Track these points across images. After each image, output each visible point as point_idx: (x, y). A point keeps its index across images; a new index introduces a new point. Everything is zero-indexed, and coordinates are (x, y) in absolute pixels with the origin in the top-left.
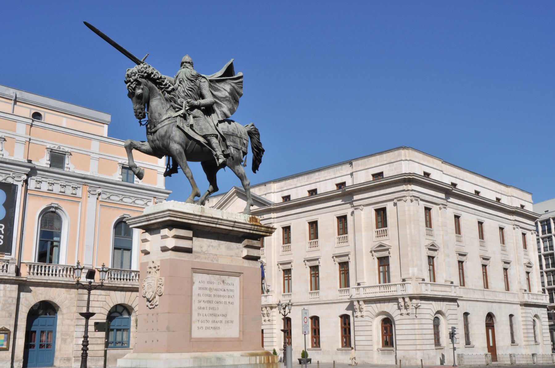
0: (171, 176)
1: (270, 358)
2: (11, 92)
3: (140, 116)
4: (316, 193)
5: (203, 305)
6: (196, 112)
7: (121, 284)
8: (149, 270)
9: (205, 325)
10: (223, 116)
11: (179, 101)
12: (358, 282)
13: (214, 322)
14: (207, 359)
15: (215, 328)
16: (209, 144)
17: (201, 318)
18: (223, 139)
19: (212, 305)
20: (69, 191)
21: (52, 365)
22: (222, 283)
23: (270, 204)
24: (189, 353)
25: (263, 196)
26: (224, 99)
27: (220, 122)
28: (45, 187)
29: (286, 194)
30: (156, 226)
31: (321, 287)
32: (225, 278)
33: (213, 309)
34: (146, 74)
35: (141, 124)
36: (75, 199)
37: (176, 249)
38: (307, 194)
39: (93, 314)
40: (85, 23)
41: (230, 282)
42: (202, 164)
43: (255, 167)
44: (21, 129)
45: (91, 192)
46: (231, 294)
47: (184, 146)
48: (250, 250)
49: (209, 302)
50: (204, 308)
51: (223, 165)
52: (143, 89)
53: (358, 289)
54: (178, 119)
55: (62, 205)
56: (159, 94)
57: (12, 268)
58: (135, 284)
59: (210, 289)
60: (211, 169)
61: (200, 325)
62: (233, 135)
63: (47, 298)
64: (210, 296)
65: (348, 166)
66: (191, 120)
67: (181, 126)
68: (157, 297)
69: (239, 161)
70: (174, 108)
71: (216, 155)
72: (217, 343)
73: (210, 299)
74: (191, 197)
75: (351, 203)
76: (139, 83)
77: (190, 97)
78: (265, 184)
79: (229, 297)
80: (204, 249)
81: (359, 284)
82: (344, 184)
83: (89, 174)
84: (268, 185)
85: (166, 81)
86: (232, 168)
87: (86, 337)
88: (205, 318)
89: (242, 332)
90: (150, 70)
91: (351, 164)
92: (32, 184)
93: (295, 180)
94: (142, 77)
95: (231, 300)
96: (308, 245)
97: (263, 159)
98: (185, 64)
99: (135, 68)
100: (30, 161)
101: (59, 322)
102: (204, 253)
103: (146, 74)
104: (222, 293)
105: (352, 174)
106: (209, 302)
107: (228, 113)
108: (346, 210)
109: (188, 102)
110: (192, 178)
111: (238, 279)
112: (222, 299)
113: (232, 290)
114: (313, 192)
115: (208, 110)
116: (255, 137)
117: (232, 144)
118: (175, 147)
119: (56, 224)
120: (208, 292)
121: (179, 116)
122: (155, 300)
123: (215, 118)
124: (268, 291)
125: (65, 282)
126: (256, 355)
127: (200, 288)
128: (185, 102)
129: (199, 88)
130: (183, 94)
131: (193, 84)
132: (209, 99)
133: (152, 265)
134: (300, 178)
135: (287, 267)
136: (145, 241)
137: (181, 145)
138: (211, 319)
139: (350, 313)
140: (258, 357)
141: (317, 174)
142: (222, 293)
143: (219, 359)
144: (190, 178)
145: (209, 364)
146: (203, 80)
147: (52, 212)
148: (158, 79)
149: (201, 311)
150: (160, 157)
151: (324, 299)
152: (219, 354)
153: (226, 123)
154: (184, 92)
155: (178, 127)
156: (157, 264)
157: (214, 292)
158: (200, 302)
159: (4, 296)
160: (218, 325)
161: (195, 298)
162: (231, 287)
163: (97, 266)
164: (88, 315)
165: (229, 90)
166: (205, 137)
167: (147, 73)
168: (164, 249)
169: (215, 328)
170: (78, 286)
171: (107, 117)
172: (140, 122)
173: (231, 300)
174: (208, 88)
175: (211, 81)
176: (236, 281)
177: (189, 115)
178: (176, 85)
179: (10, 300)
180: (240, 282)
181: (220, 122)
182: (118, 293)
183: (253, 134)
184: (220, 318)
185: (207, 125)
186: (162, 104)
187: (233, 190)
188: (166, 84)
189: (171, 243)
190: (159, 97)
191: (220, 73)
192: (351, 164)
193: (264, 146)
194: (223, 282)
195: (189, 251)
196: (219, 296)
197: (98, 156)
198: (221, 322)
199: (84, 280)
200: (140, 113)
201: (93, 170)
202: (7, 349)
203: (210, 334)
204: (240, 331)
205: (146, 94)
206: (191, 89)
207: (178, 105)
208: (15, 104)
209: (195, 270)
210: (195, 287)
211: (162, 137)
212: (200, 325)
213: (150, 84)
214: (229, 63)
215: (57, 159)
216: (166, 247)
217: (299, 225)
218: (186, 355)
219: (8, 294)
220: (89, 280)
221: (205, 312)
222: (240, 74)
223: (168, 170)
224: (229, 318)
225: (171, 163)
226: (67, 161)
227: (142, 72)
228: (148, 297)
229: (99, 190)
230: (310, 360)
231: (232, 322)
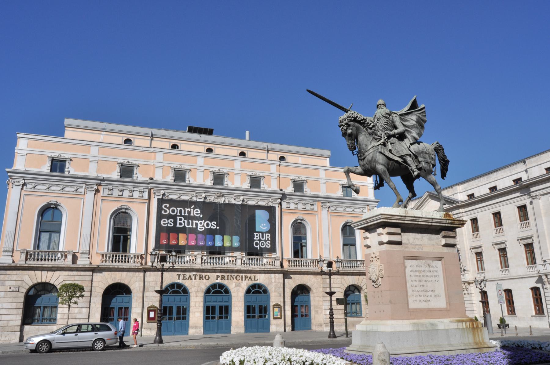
1: (475, 324)
2: (265, 145)
3: (352, 148)
4: (496, 189)
5: (415, 283)
6: (392, 139)
7: (351, 270)
8: (371, 259)
9: (418, 298)
11: (379, 134)
12: (544, 259)
13: (425, 296)
14: (423, 325)
15: (426, 301)
16: (405, 162)
17: (415, 293)
18: (415, 157)
19: (422, 284)
20: (308, 207)
21: (310, 329)
23: (458, 202)
24: (409, 321)
25: (452, 197)
26: (413, 127)
27: (412, 144)
28: (292, 206)
29: (470, 192)
30: (373, 227)
31: (510, 265)
32: (430, 262)
33: (423, 286)
36: (313, 212)
37: (390, 243)
38: (488, 191)
39: (334, 293)
40: (308, 91)
41: (434, 265)
42: (401, 177)
43: (443, 175)
44: (274, 169)
46: (436, 274)
48: (448, 239)
50: (416, 286)
51: (418, 176)
52: (352, 129)
53: (544, 265)
54: (380, 146)
55: (305, 217)
56: (364, 131)
57: (278, 263)
59: (419, 271)
60: (409, 180)
61: (414, 298)
62: (423, 152)
63: (302, 283)
64: (419, 276)
65: (522, 164)
66: (389, 146)
67: (382, 151)
68: (380, 279)
69: (430, 172)
70: (376, 139)
71: (412, 169)
72: (430, 313)
73: (420, 279)
74: (396, 203)
75: (529, 194)
76: (349, 126)
77: (387, 129)
78: (451, 187)
79: (435, 276)
80: (411, 241)
81: (545, 261)
82: (520, 179)
83: (320, 194)
84: (454, 188)
85: (367, 121)
86: (425, 177)
87: (331, 309)
88: (417, 294)
89: (449, 303)
90: (355, 115)
91: (524, 162)
92: (284, 205)
93: (477, 181)
94: (351, 121)
95: (436, 279)
96: (494, 232)
97: (449, 167)
99: (345, 115)
100: (281, 190)
101: (312, 299)
102: (411, 244)
104: (429, 274)
105: (526, 171)
106: (419, 281)
107: (417, 137)
108: (525, 200)
109: (385, 134)
110: (395, 189)
111: (440, 262)
112: (429, 279)
113: (436, 271)
114: (493, 189)
115: (401, 137)
116: (441, 152)
117: (422, 159)
118: (380, 168)
119: (303, 231)
120: (418, 273)
121: (380, 144)
122: (378, 281)
123: (407, 142)
124: (464, 270)
126: (462, 321)
127: (411, 271)
128: (383, 134)
129: (393, 122)
130: (381, 128)
132: (401, 129)
133: (373, 256)
134: (481, 179)
135: (479, 250)
136: (366, 238)
137: (384, 165)
138: (422, 294)
139: (539, 285)
140: (464, 323)
141: (495, 174)
142: (429, 274)
143: (432, 324)
145: (425, 329)
146: (395, 115)
147: (299, 223)
148: (362, 120)
149: (414, 288)
150: (370, 176)
151: (514, 275)
152: (432, 321)
153: (416, 144)
154: (381, 126)
155: (380, 152)
156: (377, 254)
157: (422, 274)
158: (412, 281)
159: (275, 282)
160: (429, 298)
161: (408, 278)
162: (435, 269)
163: (333, 258)
164: (331, 294)
165: (415, 120)
166: (401, 157)
168: (381, 243)
169: (426, 301)
170: (322, 273)
171: (328, 153)
172: (353, 153)
173: (436, 279)
174: (399, 121)
175: (401, 115)
176: (439, 263)
177: (388, 142)
178: (375, 122)
179: (279, 285)
180: (442, 264)
181: (412, 144)
182: (350, 277)
183: (439, 150)
184: (430, 293)
185: (402, 148)
186: (367, 137)
187: (427, 194)
188: (368, 123)
189: (386, 238)
190: (364, 133)
191: (407, 108)
192: (524, 162)
194: (429, 265)
195: (399, 243)
197: (325, 181)
198: (431, 296)
199: (325, 269)
200: (352, 146)
201: (323, 192)
202: (280, 318)
203: (423, 305)
204: (447, 303)
205: (355, 132)
206: (387, 124)
208: (268, 152)
209: (406, 257)
210: (408, 270)
211: (370, 162)
212: (414, 298)
213: (357, 124)
214: (413, 99)
215: (299, 186)
216: (382, 241)
217: (485, 216)
218: (406, 322)
219: (277, 281)
220: (329, 269)
221: (417, 289)
222: (423, 106)
224: (436, 293)
225: (378, 180)
226: (305, 187)
227: (350, 117)
228: (373, 279)
229: (329, 205)
230: (508, 325)
231: (439, 296)
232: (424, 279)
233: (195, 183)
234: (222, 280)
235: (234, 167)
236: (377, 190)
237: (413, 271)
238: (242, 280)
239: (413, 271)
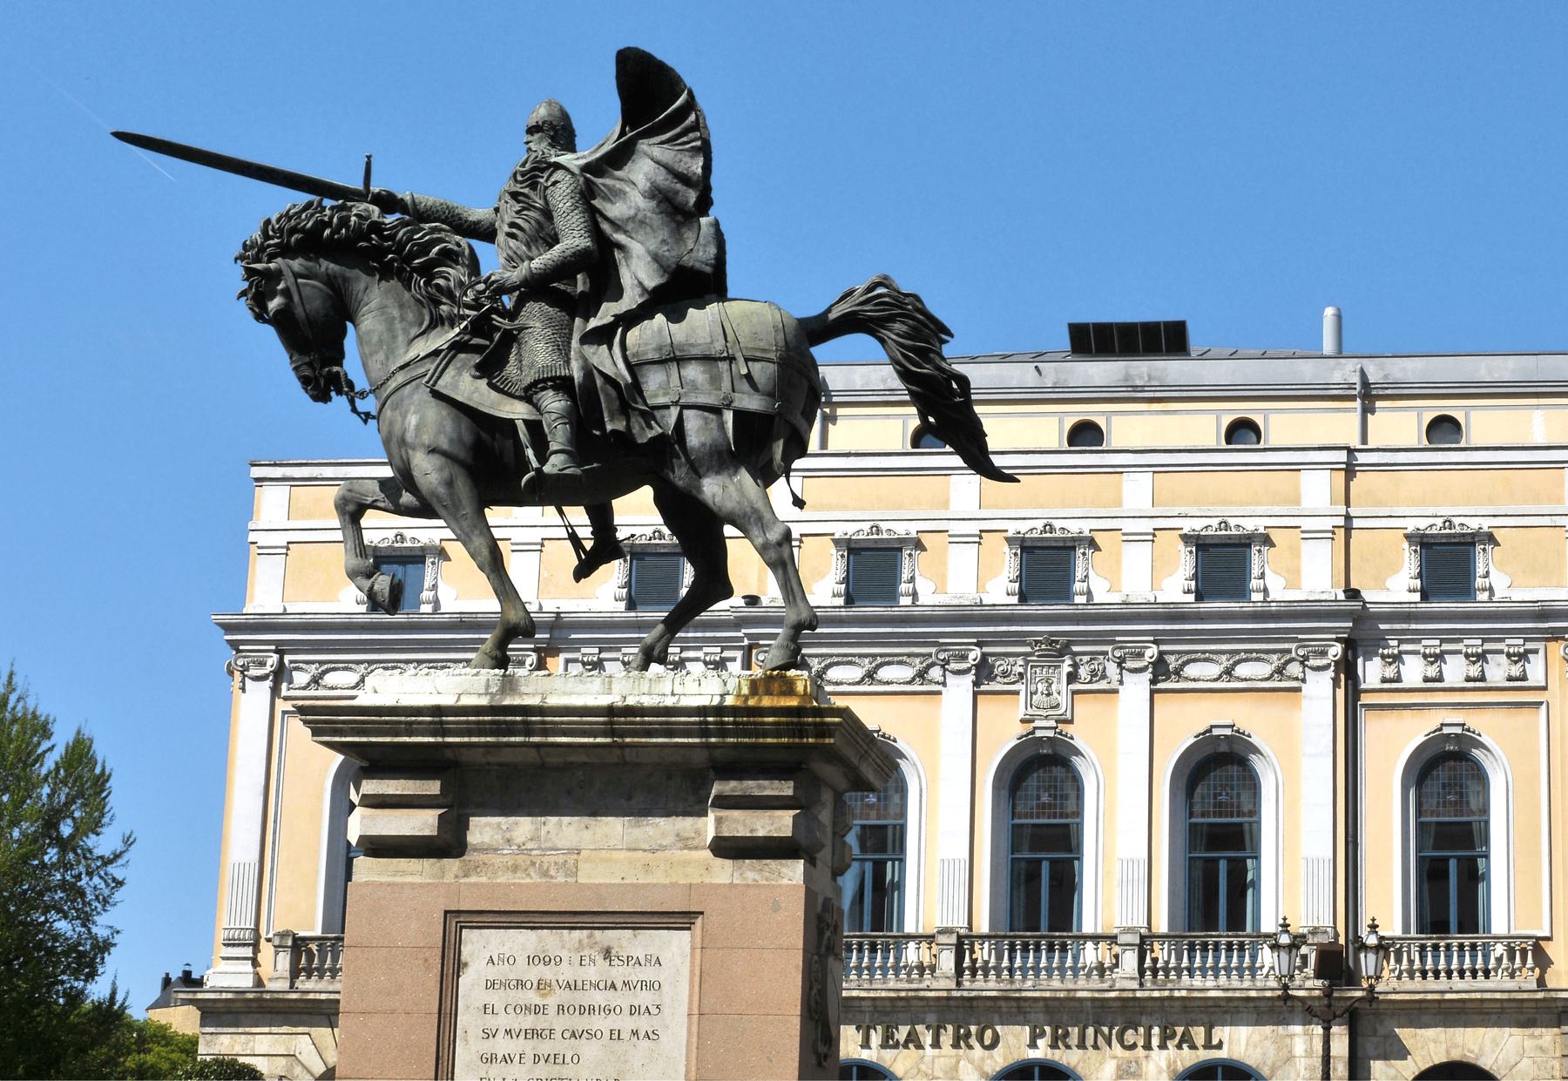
5: (502, 1045)
7: (1460, 988)
19: (545, 1047)
22: (599, 959)
28: (1414, 670)
45: (1312, 662)
46: (644, 998)
49: (535, 1034)
50: (507, 1059)
58: (935, 985)
59: (542, 986)
63: (1456, 1055)
64: (538, 1010)
73: (540, 1023)
79: (634, 1010)
95: (643, 1024)
104: (598, 998)
106: (535, 1034)
113: (648, 985)
119: (1070, 806)
120: (532, 997)
125: (1505, 996)
137: (444, 454)
142: (598, 998)
158: (489, 1035)
173: (643, 1024)
176: (675, 946)
194: (607, 953)
196: (583, 1010)
199: (1308, 985)
208: (1367, 410)
215: (1447, 560)
232: (560, 1023)
233: (1116, 598)
234: (1054, 1046)
235: (1119, 504)
237: (506, 985)
238: (1148, 1047)
239: (506, 985)
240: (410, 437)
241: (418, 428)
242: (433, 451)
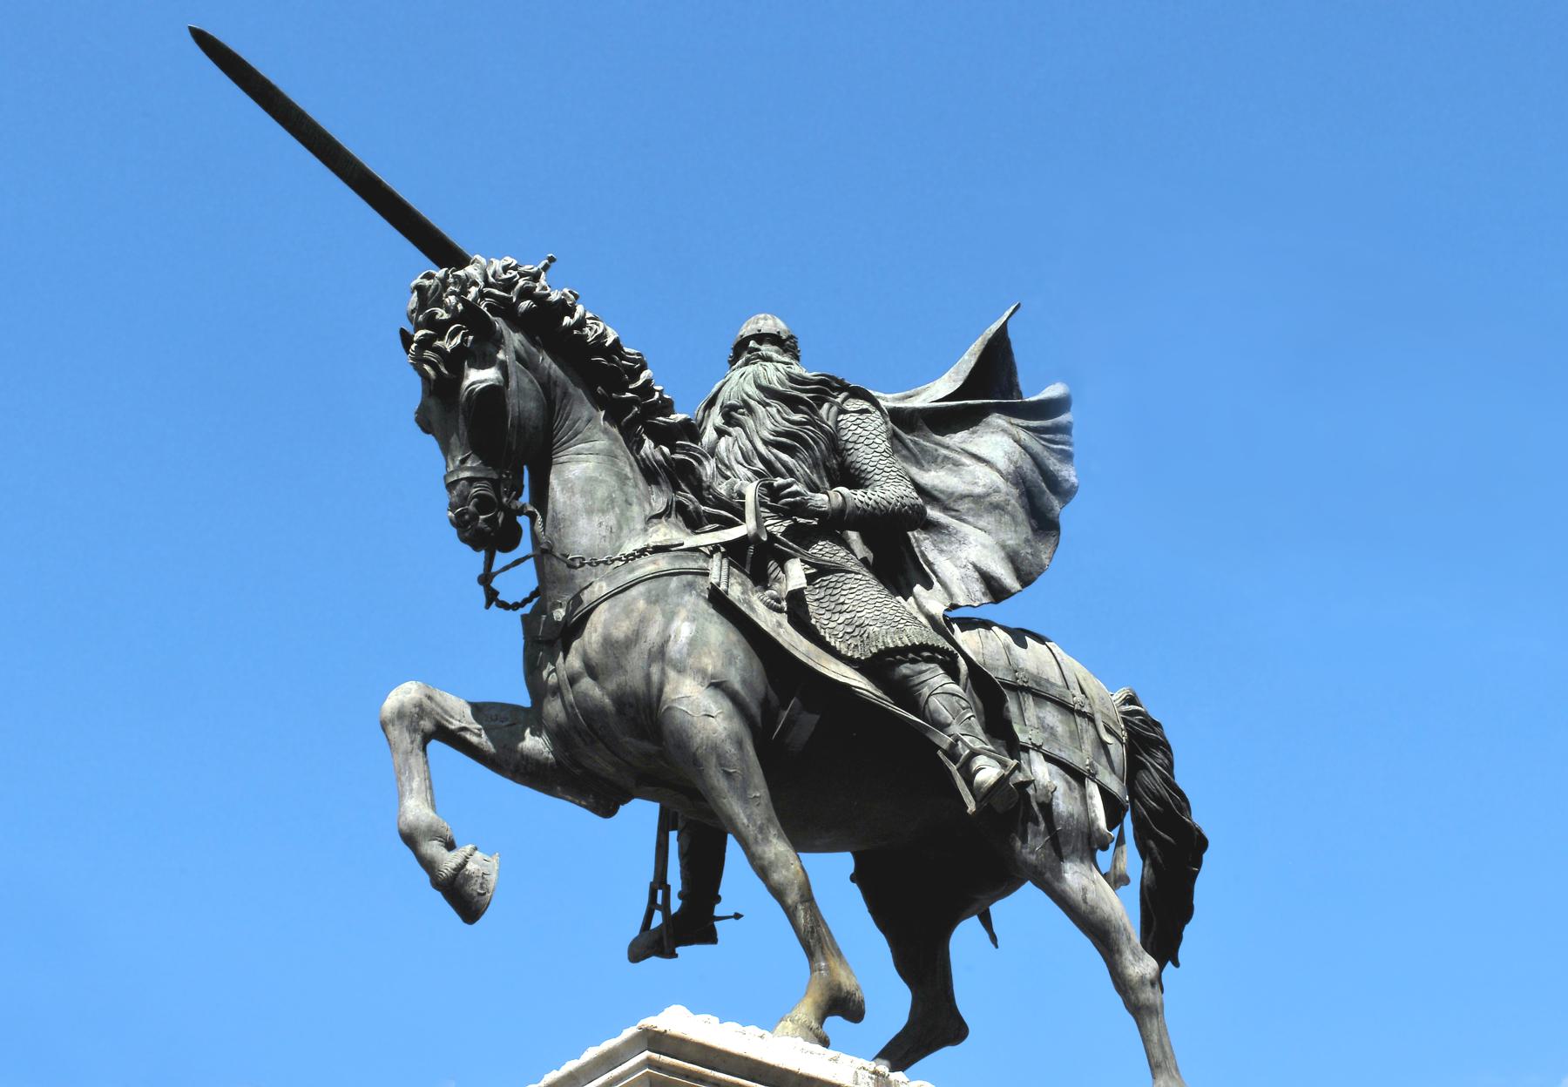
0: (673, 955)
3: (487, 526)
10: (978, 588)
26: (982, 503)
34: (525, 304)
35: (492, 597)
47: (755, 709)
74: (805, 1011)
97: (1206, 888)
98: (752, 344)
103: (525, 304)
110: (807, 897)
116: (1153, 761)
118: (701, 710)
131: (797, 417)
137: (733, 697)
144: (793, 897)
150: (606, 808)
155: (718, 600)
165: (1002, 463)
167: (541, 300)
172: (486, 579)
175: (903, 420)
186: (622, 479)
193: (1200, 816)
206: (789, 442)
207: (719, 502)
211: (616, 648)
214: (995, 327)
222: (1053, 391)
223: (657, 920)
227: (509, 285)
236: (654, 961)
240: (673, 650)
241: (692, 642)
242: (718, 685)
